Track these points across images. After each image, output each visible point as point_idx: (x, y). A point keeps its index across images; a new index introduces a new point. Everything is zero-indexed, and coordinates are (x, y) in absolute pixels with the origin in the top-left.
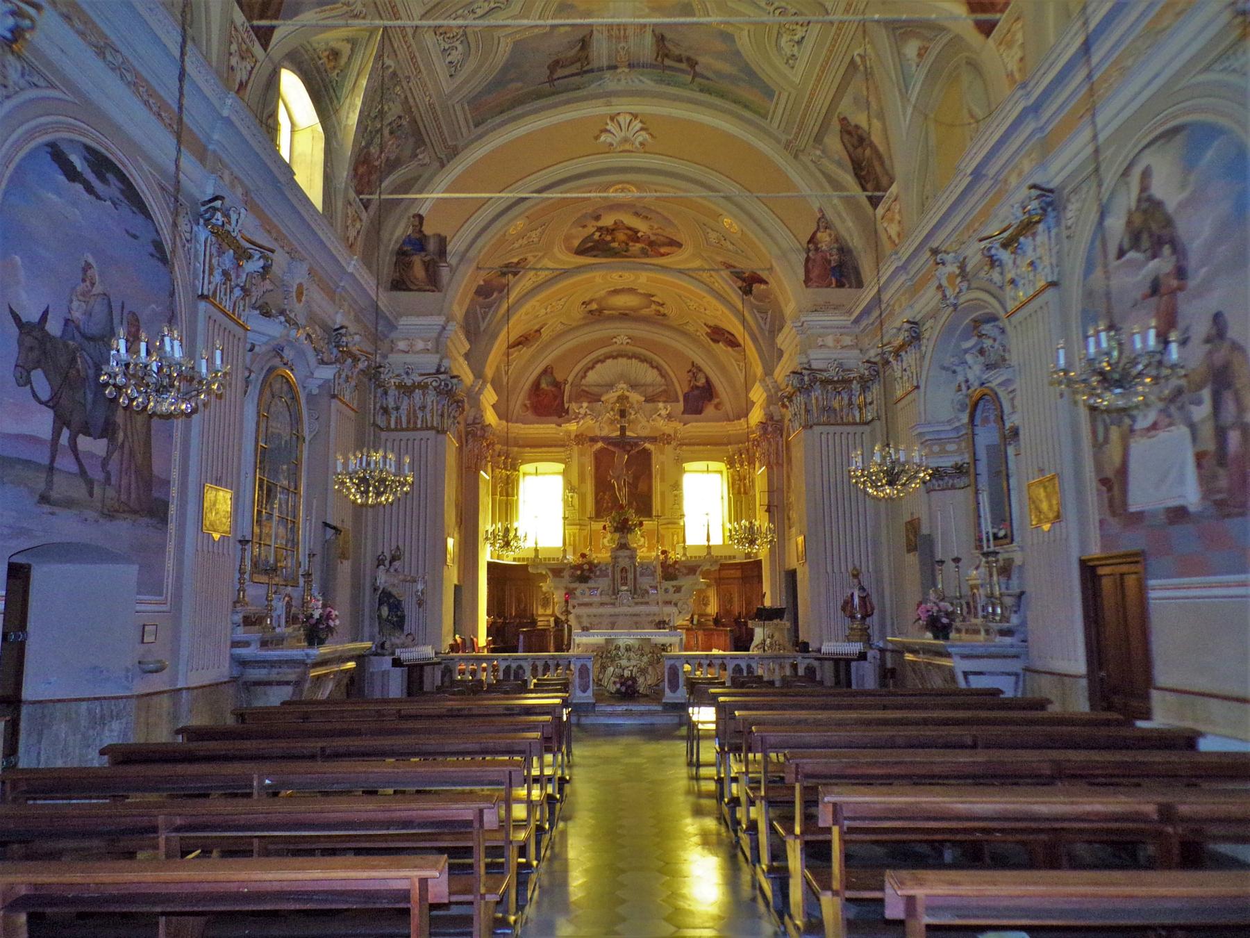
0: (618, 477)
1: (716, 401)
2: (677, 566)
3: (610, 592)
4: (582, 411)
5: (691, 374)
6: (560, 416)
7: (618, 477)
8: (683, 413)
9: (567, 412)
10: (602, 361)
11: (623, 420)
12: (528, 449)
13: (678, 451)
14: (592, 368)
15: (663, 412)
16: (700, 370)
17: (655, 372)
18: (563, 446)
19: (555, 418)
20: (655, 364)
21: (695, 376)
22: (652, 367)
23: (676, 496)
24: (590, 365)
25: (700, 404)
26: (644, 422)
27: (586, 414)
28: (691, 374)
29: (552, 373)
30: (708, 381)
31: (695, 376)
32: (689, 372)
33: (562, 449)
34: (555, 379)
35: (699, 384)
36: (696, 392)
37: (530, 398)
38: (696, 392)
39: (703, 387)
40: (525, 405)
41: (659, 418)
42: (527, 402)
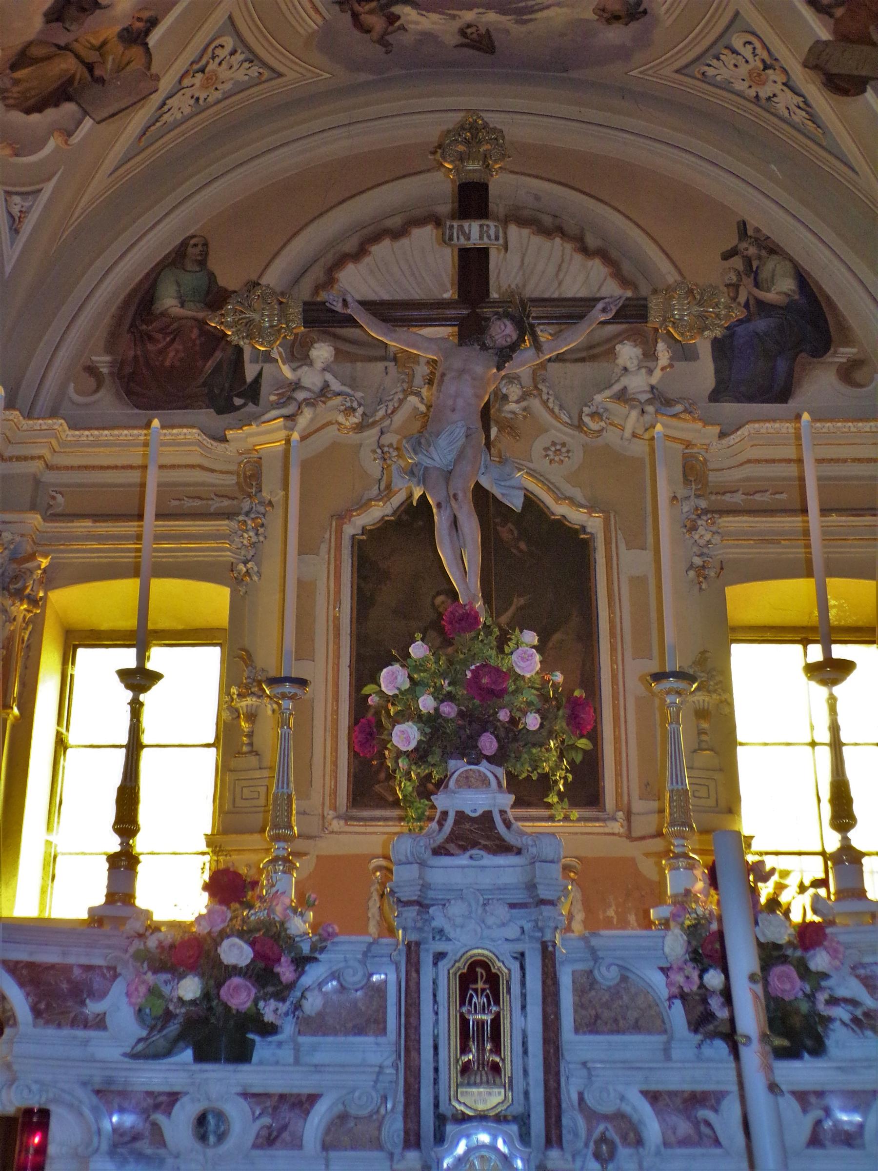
0: (448, 475)
1: (844, 354)
2: (819, 961)
3: (394, 1127)
4: (311, 378)
5: (737, 262)
6: (225, 408)
7: (448, 475)
8: (715, 396)
9: (253, 392)
10: (397, 234)
11: (474, 227)
12: (84, 526)
13: (703, 534)
14: (359, 254)
15: (637, 383)
16: (773, 250)
17: (597, 267)
18: (229, 515)
19: (206, 415)
20: (592, 242)
21: (751, 270)
22: (584, 250)
23: (701, 714)
24: (351, 245)
25: (782, 365)
26: (559, 432)
27: (324, 392)
28: (737, 262)
29: (202, 263)
30: (803, 280)
31: (751, 270)
32: (727, 256)
33: (224, 525)
34: (212, 276)
35: (770, 297)
36: (761, 325)
37: (111, 344)
38: (761, 325)
39: (790, 307)
40: (91, 370)
41: (620, 409)
42: (103, 361)
